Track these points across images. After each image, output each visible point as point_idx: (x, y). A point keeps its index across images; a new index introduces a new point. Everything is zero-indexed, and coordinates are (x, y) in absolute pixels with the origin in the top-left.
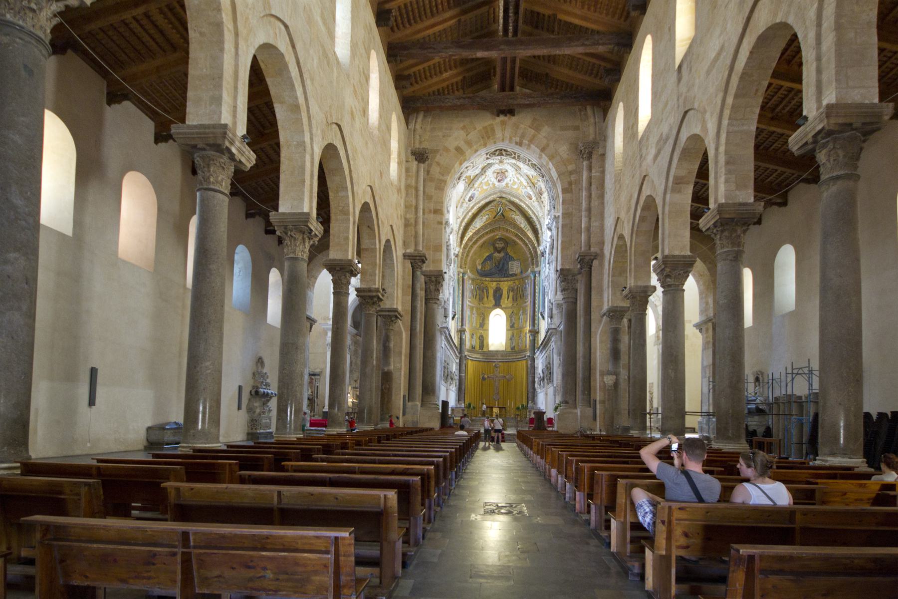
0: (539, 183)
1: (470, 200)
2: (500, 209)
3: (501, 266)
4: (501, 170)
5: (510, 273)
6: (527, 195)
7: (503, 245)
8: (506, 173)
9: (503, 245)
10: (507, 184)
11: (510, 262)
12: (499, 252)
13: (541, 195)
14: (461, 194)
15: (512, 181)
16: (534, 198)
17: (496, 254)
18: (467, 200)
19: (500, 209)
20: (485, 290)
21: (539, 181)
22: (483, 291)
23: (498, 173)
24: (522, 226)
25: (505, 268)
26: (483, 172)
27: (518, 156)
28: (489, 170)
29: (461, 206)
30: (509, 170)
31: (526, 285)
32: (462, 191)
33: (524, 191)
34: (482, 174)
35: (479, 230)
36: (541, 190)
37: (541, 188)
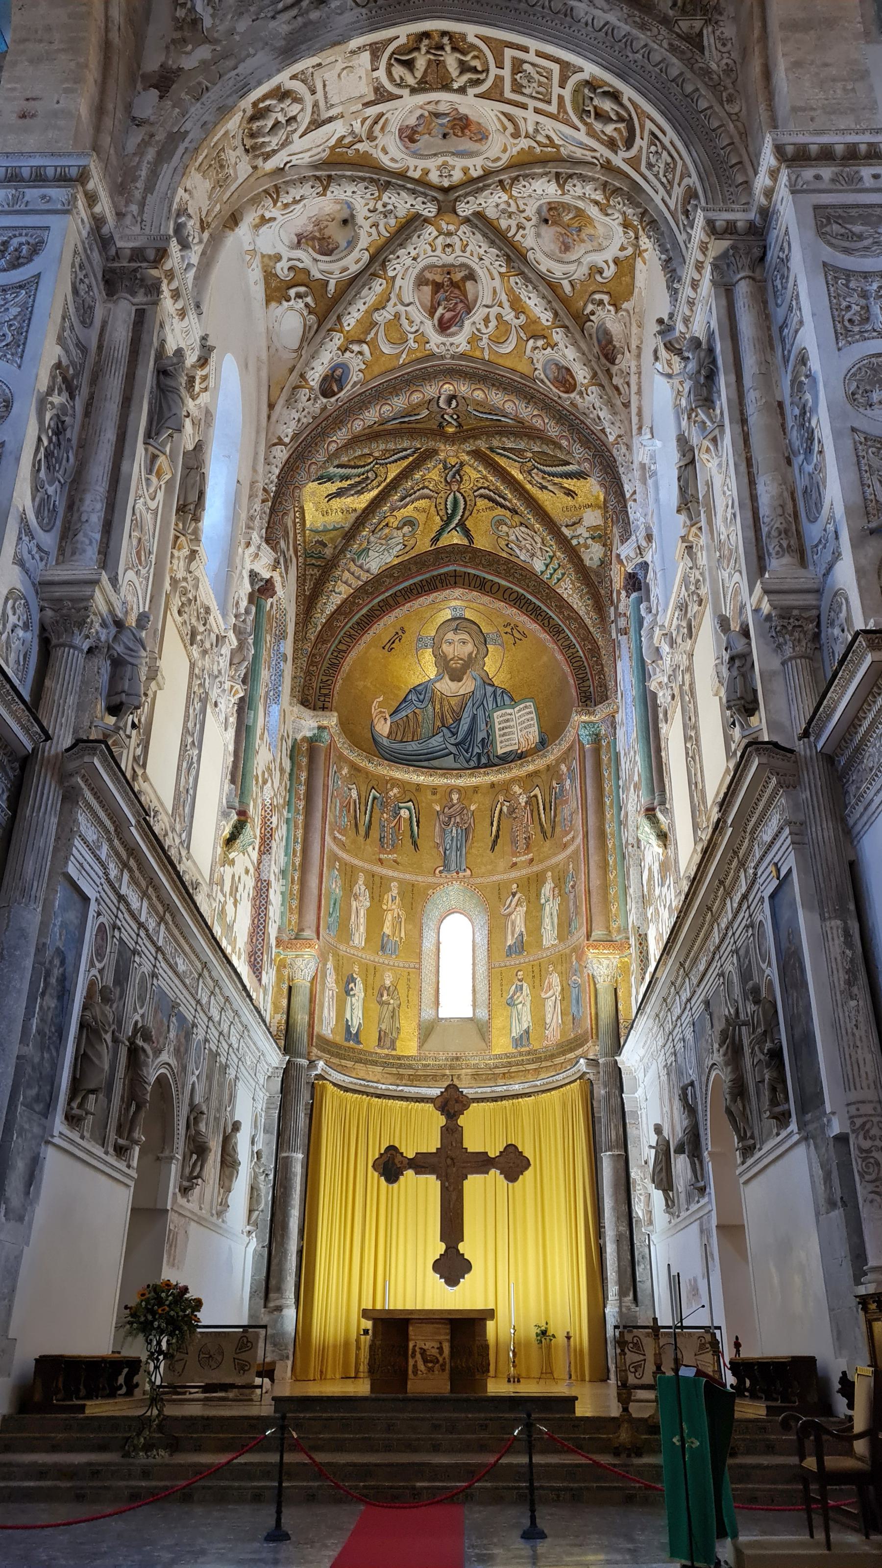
0: (601, 313)
1: (327, 392)
2: (455, 502)
3: (464, 726)
4: (448, 269)
5: (500, 752)
6: (552, 372)
7: (469, 647)
8: (469, 285)
9: (469, 647)
10: (474, 340)
11: (499, 713)
12: (456, 676)
13: (613, 363)
14: (288, 357)
15: (493, 323)
16: (581, 374)
17: (446, 687)
18: (316, 375)
19: (455, 502)
20: (405, 813)
21: (601, 303)
22: (396, 813)
23: (437, 287)
24: (538, 565)
25: (481, 735)
26: (376, 266)
27: (517, 66)
28: (401, 252)
29: (291, 402)
30: (481, 272)
31: (560, 782)
32: (296, 347)
33: (541, 357)
34: (375, 275)
35: (377, 582)
36: (610, 341)
37: (607, 333)
